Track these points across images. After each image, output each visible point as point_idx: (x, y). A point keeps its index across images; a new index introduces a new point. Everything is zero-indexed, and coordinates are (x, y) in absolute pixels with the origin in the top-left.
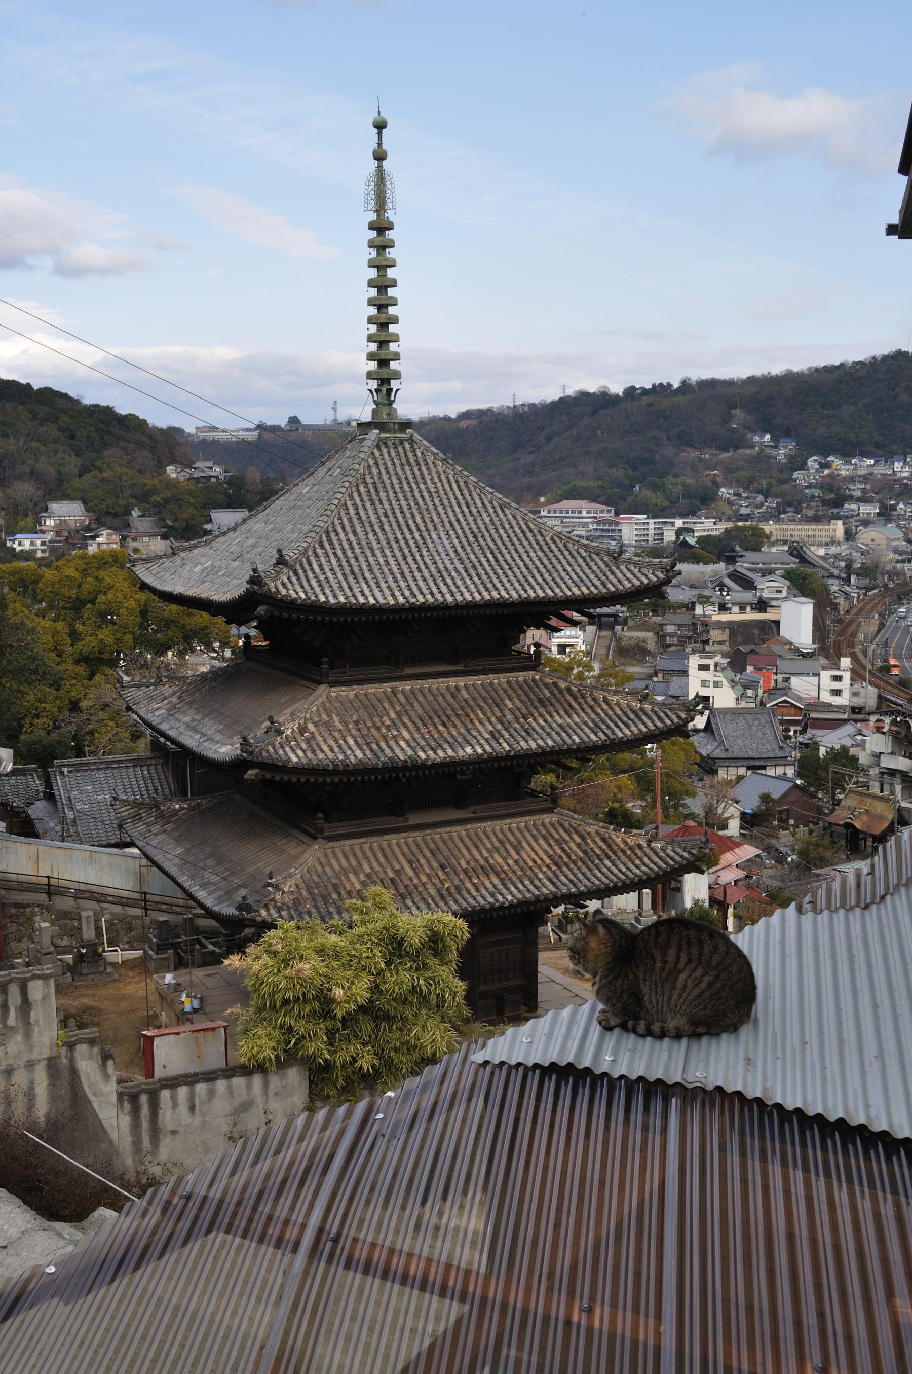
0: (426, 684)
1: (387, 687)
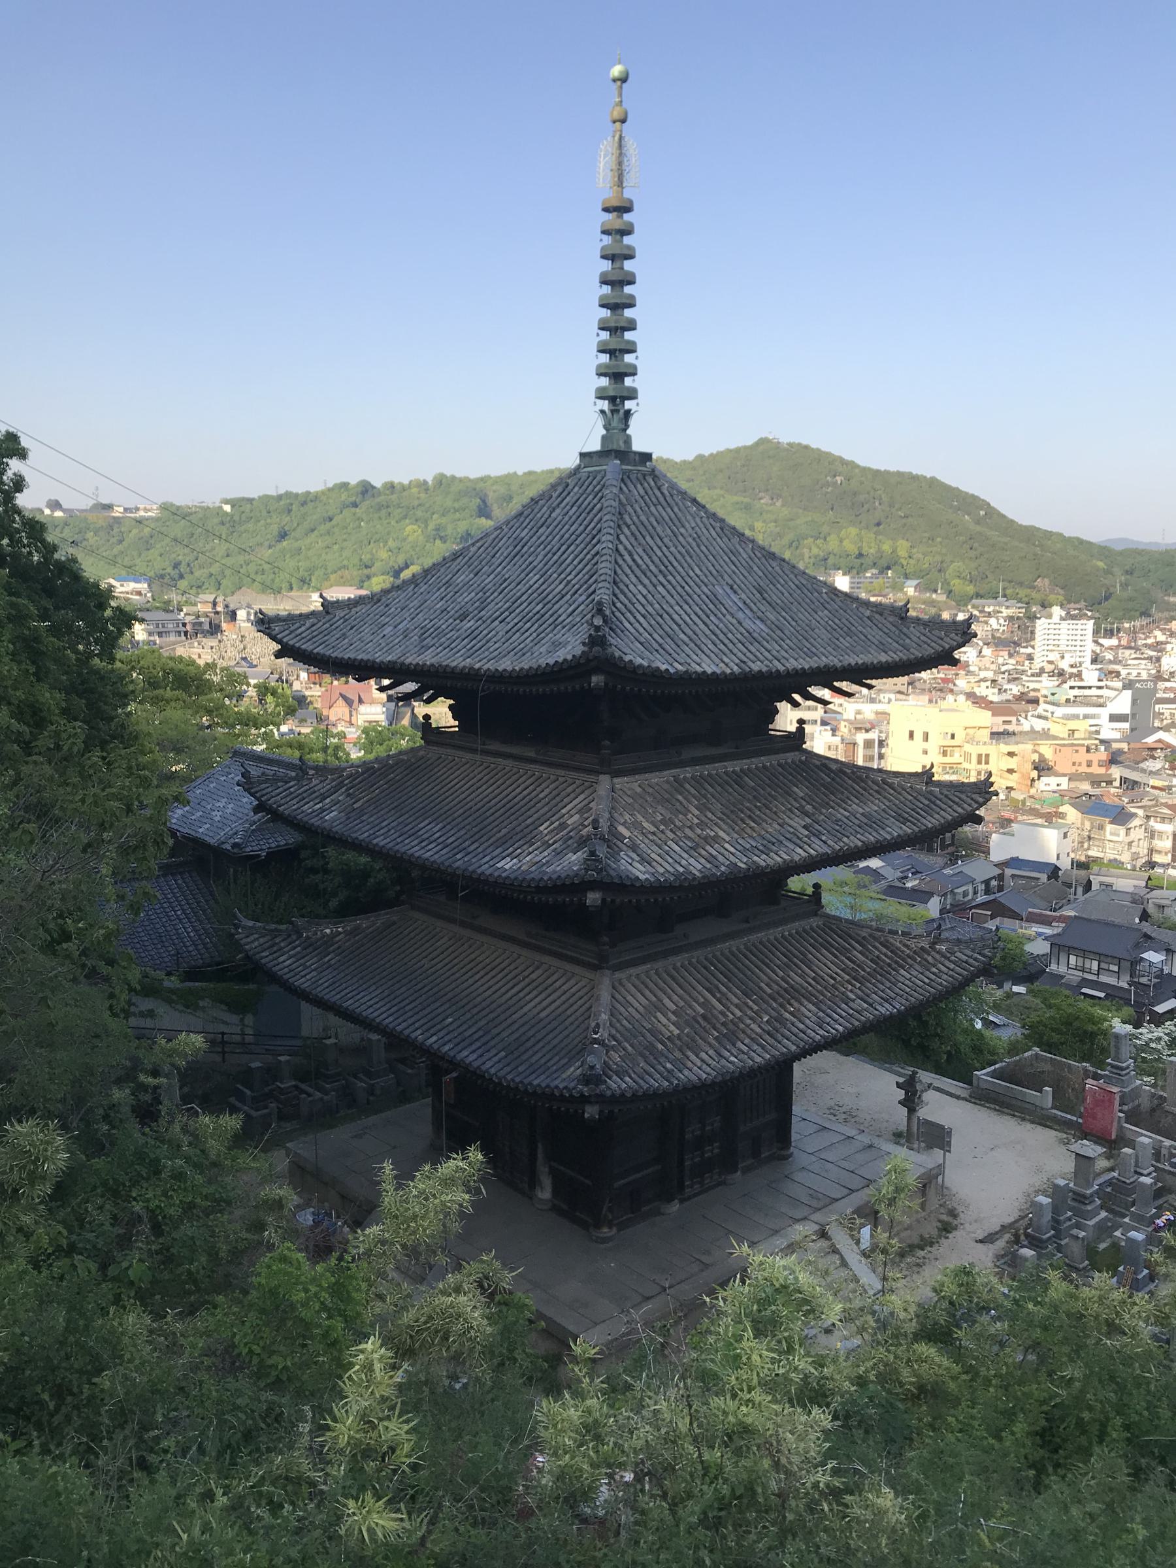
0: (707, 769)
1: (669, 774)
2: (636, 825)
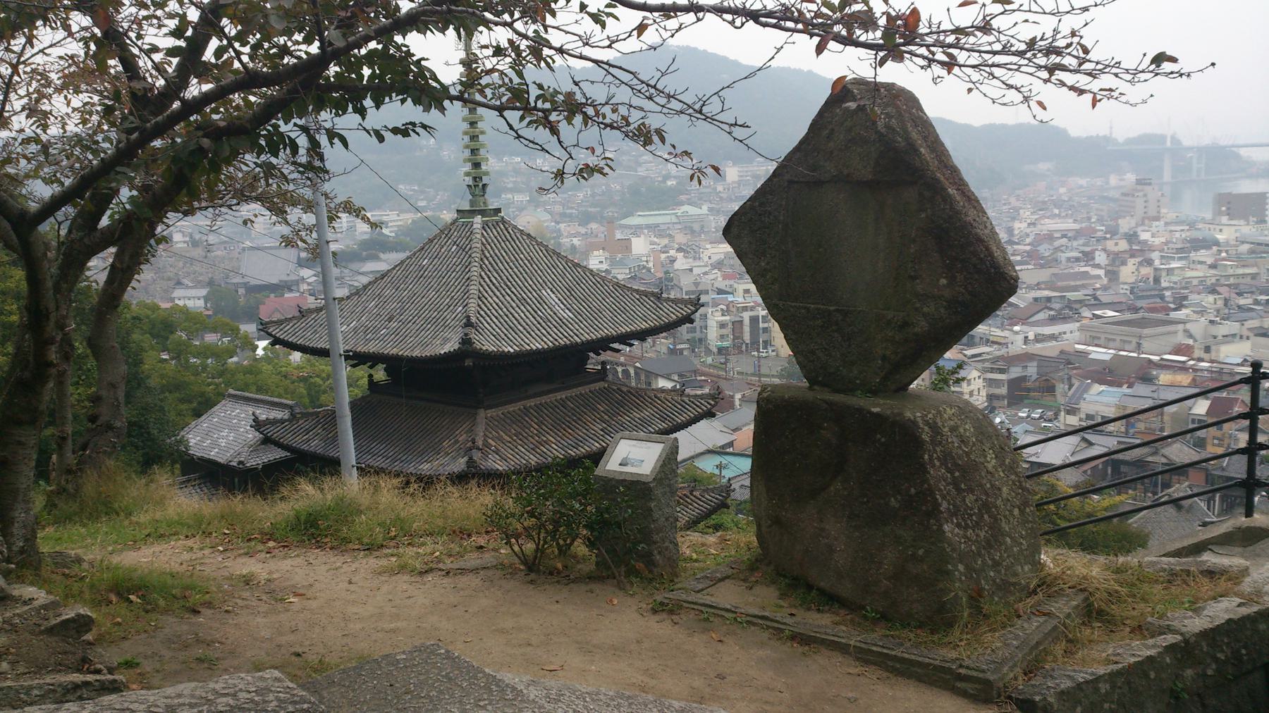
0: (544, 399)
1: (520, 405)
2: (500, 439)
